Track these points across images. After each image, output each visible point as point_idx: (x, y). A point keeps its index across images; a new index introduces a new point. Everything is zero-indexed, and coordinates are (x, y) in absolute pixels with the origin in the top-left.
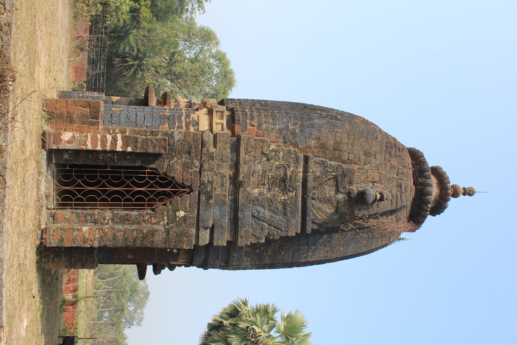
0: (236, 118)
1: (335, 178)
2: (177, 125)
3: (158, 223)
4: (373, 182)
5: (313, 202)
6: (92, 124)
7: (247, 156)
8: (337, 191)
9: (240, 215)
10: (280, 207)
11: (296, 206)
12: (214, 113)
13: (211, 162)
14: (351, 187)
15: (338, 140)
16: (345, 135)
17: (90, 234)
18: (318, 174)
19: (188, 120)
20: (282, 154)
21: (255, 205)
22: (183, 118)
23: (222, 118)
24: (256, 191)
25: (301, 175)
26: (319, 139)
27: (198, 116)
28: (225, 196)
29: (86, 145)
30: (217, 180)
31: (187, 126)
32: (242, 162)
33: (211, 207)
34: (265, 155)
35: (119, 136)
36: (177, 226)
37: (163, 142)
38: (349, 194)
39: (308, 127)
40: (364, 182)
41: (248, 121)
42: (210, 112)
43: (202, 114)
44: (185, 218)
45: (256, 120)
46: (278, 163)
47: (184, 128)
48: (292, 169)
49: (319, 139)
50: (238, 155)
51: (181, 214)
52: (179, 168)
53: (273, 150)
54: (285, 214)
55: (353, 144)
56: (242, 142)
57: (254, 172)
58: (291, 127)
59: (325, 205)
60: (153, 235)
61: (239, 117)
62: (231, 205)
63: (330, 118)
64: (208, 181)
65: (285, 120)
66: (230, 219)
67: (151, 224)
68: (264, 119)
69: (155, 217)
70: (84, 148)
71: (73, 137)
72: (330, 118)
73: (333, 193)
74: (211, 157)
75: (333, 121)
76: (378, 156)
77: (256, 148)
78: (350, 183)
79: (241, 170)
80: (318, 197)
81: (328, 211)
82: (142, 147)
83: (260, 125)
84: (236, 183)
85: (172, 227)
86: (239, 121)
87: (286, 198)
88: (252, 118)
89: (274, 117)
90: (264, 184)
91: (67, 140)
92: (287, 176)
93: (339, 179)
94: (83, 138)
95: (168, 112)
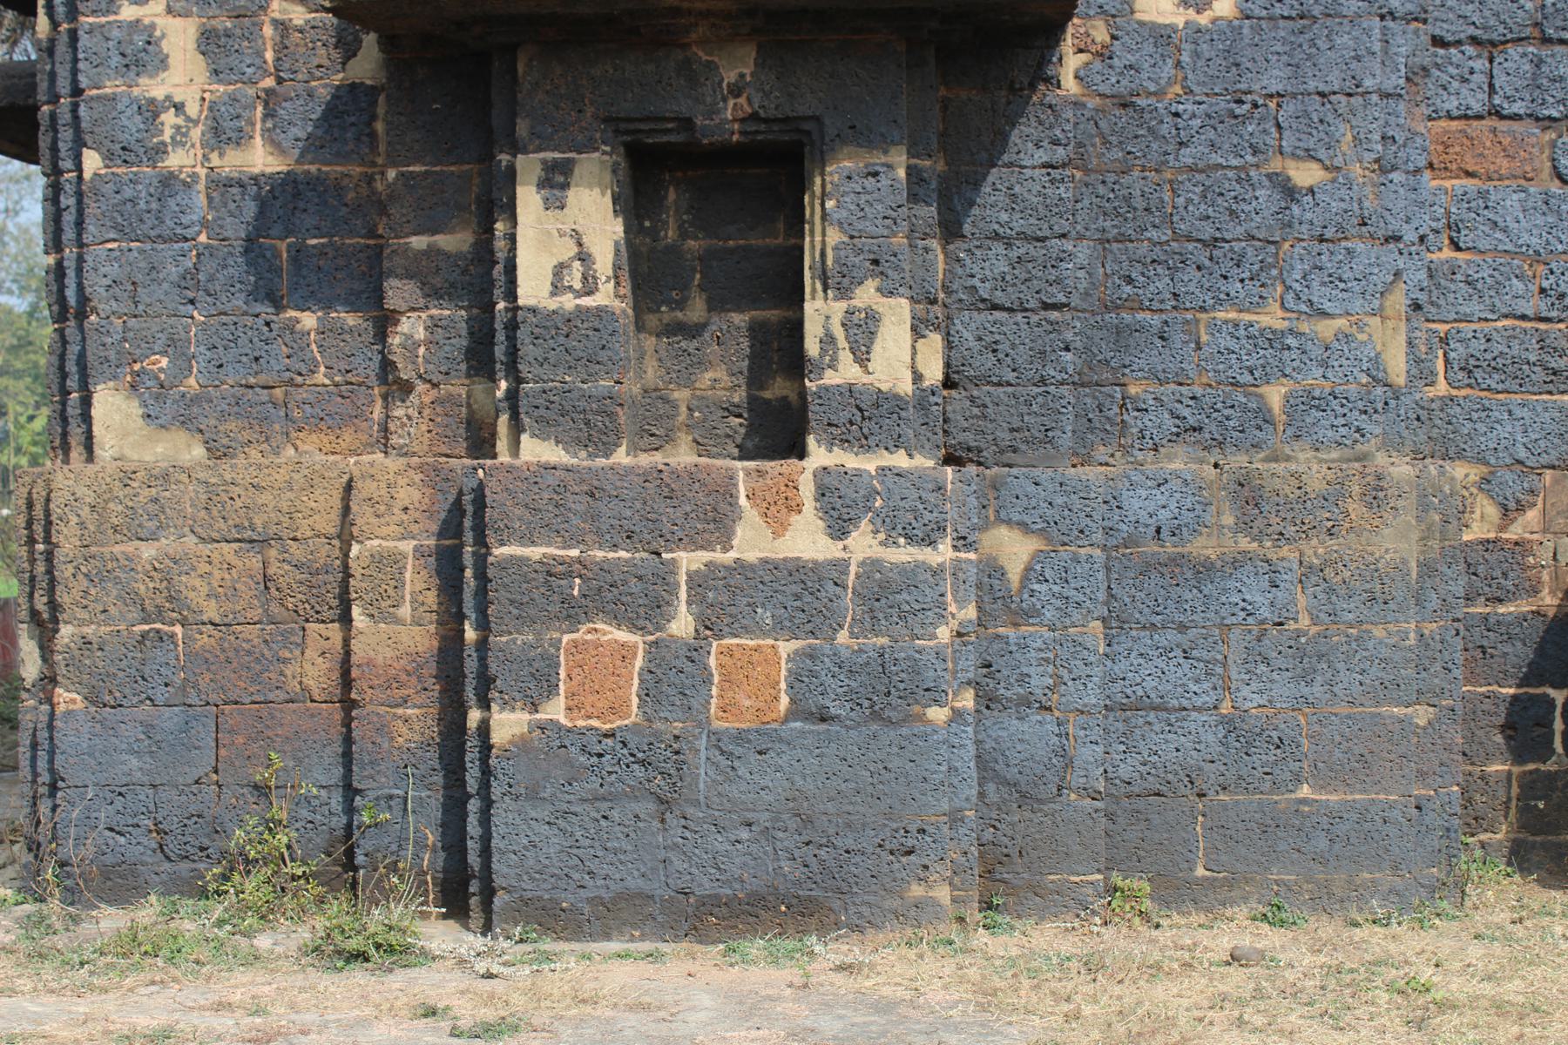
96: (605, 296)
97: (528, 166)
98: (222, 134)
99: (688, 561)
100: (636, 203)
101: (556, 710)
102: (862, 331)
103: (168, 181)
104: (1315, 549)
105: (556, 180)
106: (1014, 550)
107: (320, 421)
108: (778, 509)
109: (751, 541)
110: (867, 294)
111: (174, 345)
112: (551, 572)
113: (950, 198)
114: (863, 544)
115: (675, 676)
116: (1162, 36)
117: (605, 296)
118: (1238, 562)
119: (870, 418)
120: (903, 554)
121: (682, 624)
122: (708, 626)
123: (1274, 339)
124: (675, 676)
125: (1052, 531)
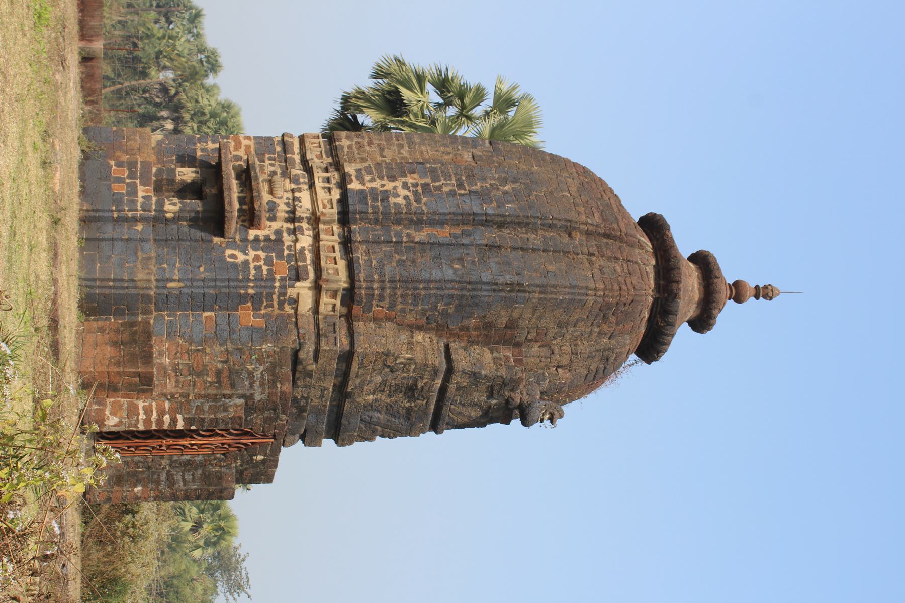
0: (357, 298)
1: (492, 387)
2: (265, 303)
3: (228, 467)
4: (558, 367)
5: (453, 407)
6: (144, 391)
7: (361, 371)
8: (491, 396)
9: (344, 421)
10: (403, 412)
11: (425, 412)
12: (323, 293)
13: (308, 379)
14: (513, 394)
15: (516, 315)
16: (530, 310)
17: (143, 493)
18: (465, 384)
19: (282, 298)
20: (413, 367)
21: (368, 410)
22: (275, 297)
23: (334, 296)
24: (371, 397)
25: (439, 386)
26: (484, 317)
27: (298, 294)
28: (325, 406)
29: (136, 426)
30: (315, 393)
31: (281, 305)
32: (353, 374)
33: (304, 419)
34: (389, 367)
35: (179, 417)
36: (253, 467)
37: (238, 420)
38: (507, 402)
39: (469, 306)
40: (543, 369)
41: (374, 302)
42: (317, 288)
43: (304, 287)
44: (263, 462)
45: (387, 301)
46: (406, 375)
47: (276, 306)
48: (425, 381)
49: (484, 317)
50: (349, 367)
51: (260, 457)
52: (259, 421)
53: (402, 363)
54: (409, 419)
55: (539, 318)
56: (356, 357)
57: (370, 382)
58: (440, 306)
59: (469, 409)
60: (221, 492)
61: (361, 298)
62: (331, 411)
63: (510, 291)
64: (302, 397)
65: (433, 300)
66: (328, 421)
67: (221, 467)
68: (400, 300)
69: (225, 461)
70: (134, 429)
71: (121, 422)
72: (510, 291)
73: (483, 398)
74: (309, 375)
75: (513, 295)
76: (580, 324)
77: (376, 360)
78: (513, 390)
79: (350, 383)
80: (460, 403)
81: (472, 414)
82: (209, 425)
83: (392, 306)
84: (342, 392)
85: (246, 469)
86: (359, 303)
87: (413, 404)
88: (381, 298)
89: (416, 298)
90: (383, 391)
91: (112, 424)
92: (416, 386)
93: (496, 388)
94: (133, 422)
95: (253, 288)
96: (178, 178)
97: (198, 170)
98: (202, 150)
99: (138, 181)
100: (193, 183)
101: (114, 168)
102: (174, 204)
103: (195, 144)
104: (139, 267)
105: (196, 172)
106: (139, 227)
107: (158, 159)
108: (147, 191)
109: (140, 188)
110: (180, 205)
111: (169, 144)
112: (136, 168)
113: (195, 221)
114: (140, 200)
115: (120, 180)
116: (224, 252)
117: (178, 178)
118: (137, 257)
119: (161, 204)
120: (139, 204)
121: (128, 181)
122: (128, 184)
123: (174, 265)
124: (120, 180)
125: (141, 232)
